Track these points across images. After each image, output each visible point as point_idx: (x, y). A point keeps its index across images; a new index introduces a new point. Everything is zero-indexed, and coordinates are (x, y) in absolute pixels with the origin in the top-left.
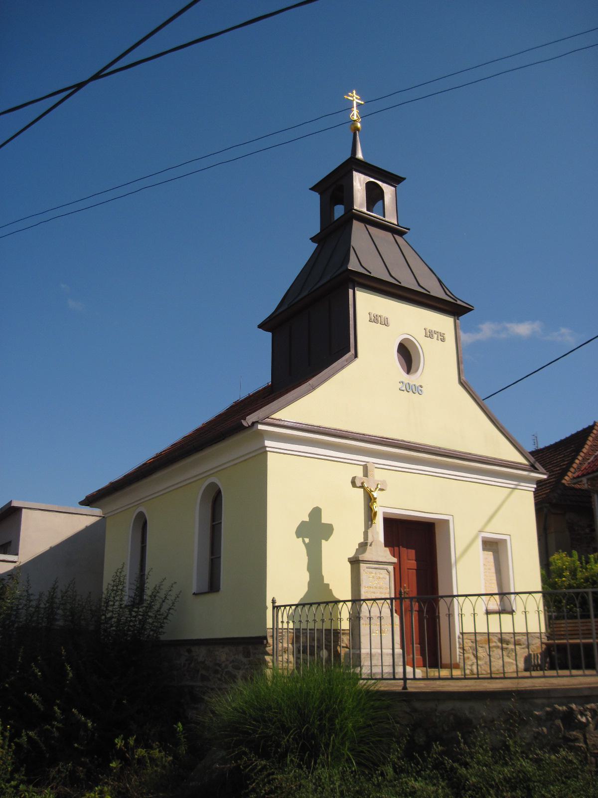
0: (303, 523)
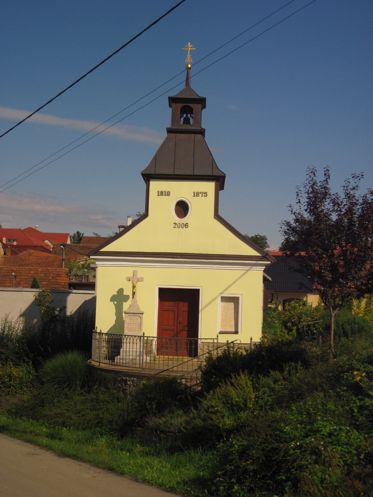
0: (114, 295)
